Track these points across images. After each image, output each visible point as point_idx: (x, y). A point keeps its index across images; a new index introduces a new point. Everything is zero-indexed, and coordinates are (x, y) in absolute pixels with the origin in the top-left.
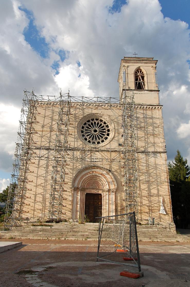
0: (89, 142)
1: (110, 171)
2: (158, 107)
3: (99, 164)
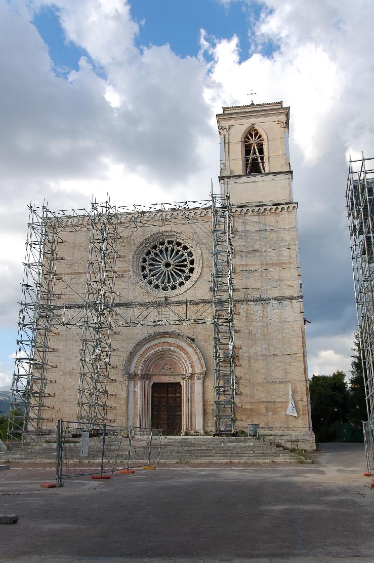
0: (157, 287)
1: (193, 340)
2: (289, 207)
3: (173, 328)
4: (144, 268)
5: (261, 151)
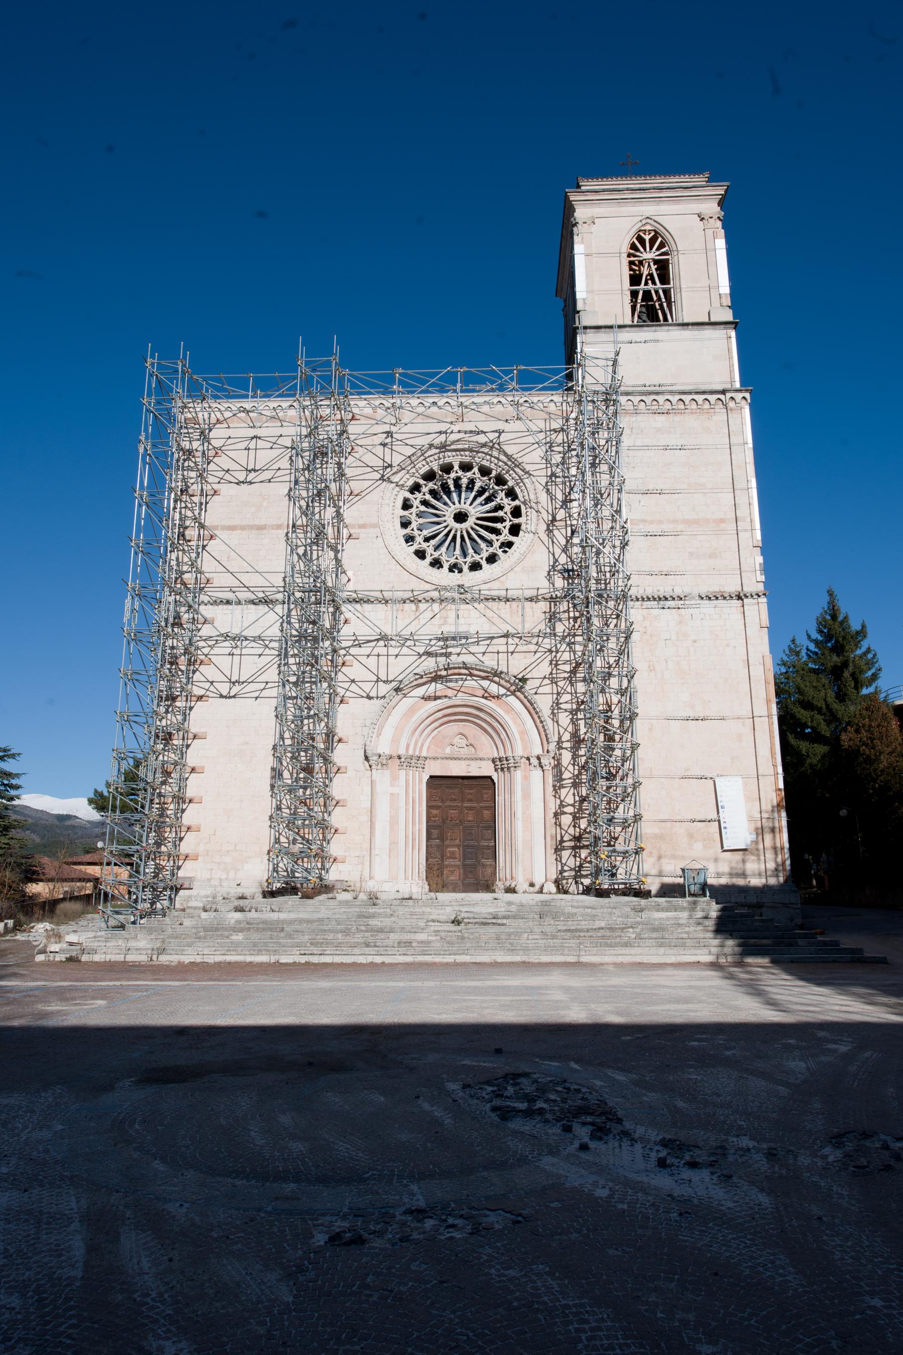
0: (436, 563)
4: (405, 524)
5: (664, 278)
